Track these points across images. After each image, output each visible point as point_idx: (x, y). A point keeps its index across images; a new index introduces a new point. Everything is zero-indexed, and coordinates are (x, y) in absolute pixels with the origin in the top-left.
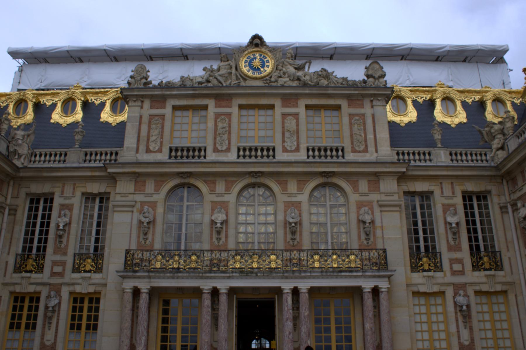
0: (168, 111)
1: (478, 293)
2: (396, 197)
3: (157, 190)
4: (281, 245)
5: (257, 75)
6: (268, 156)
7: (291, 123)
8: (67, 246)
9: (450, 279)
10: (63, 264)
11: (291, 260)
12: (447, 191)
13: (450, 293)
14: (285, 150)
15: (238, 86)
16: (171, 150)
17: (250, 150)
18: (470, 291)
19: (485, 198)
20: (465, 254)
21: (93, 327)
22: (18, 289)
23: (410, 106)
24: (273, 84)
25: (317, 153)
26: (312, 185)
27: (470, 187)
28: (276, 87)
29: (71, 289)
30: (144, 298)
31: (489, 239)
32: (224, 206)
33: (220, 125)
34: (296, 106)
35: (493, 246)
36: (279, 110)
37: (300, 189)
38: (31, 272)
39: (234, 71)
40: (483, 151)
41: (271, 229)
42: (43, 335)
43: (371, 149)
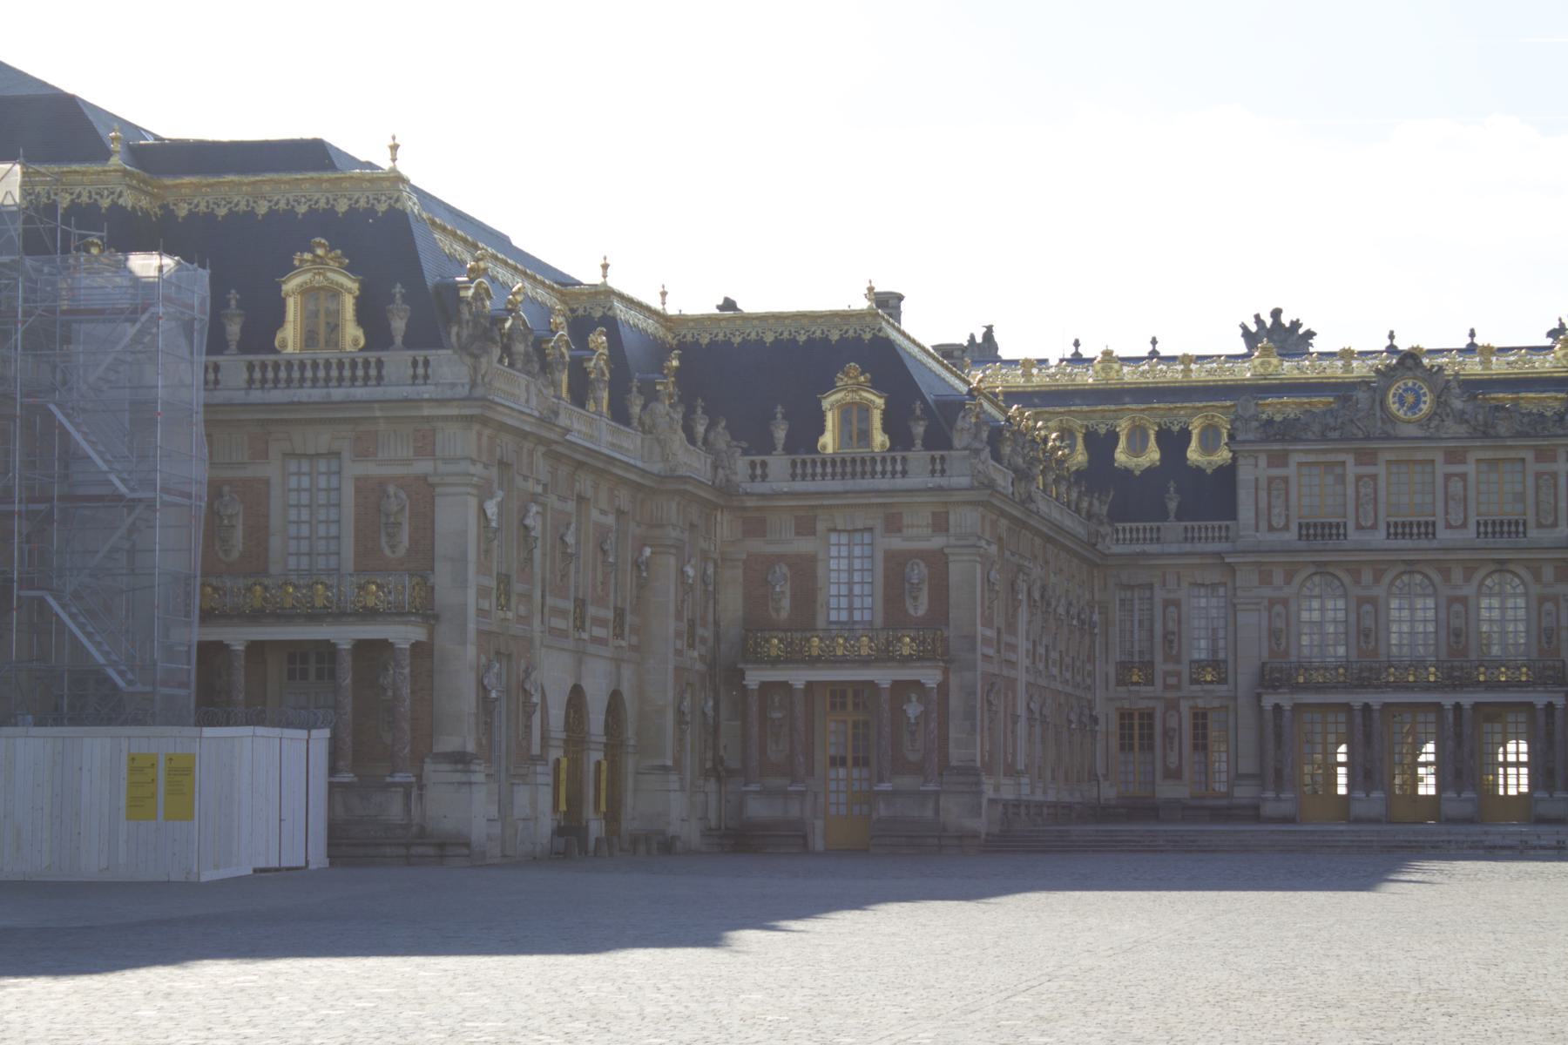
5: (1410, 416)
6: (1427, 534)
7: (1456, 487)
11: (1452, 668)
14: (1449, 526)
15: (1388, 437)
17: (1404, 525)
22: (1127, 706)
25: (1490, 529)
29: (1191, 703)
32: (1373, 601)
33: (1363, 491)
34: (1463, 462)
36: (1441, 469)
37: (1467, 579)
38: (1137, 684)
39: (1378, 408)
42: (1165, 757)
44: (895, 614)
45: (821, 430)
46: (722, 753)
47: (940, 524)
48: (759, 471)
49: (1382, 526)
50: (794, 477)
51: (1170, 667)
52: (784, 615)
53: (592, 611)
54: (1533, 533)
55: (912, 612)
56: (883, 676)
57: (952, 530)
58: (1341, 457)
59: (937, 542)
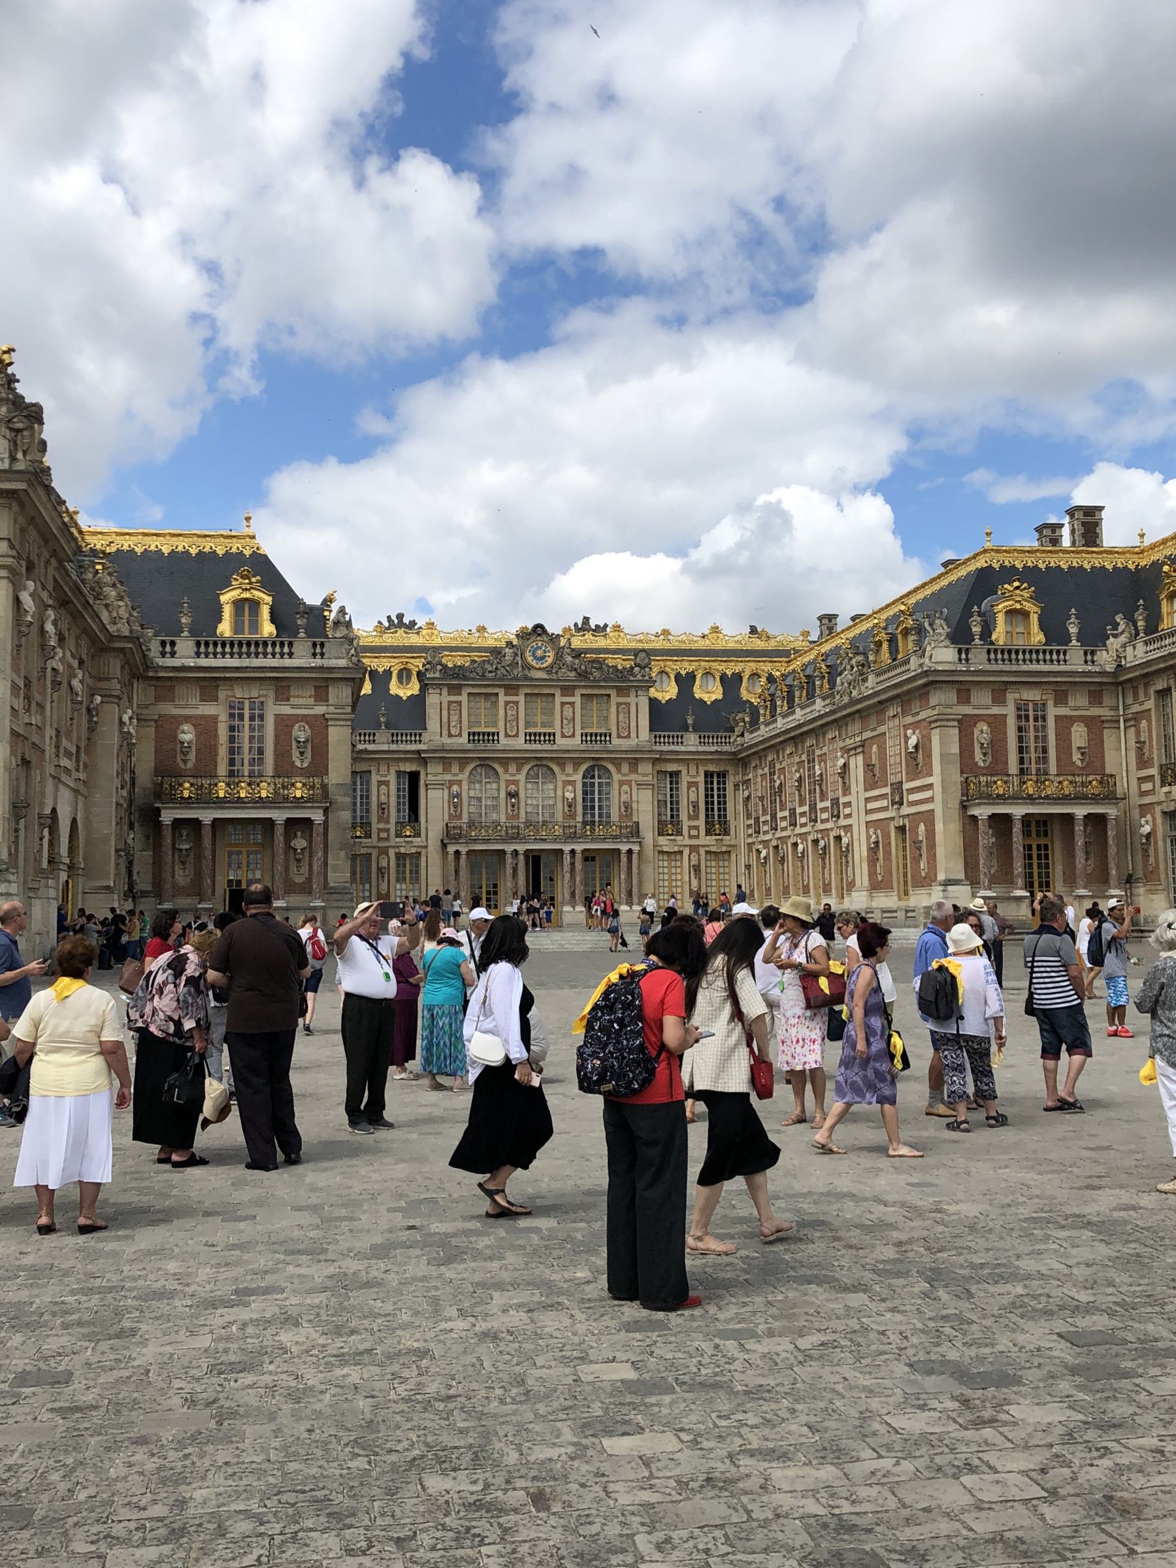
0: (464, 698)
1: (707, 852)
2: (650, 777)
3: (461, 770)
4: (559, 817)
7: (568, 711)
8: (389, 815)
9: (687, 841)
10: (388, 830)
12: (693, 771)
13: (686, 852)
14: (563, 736)
16: (469, 734)
17: (535, 735)
18: (702, 851)
19: (724, 776)
20: (701, 822)
21: (415, 878)
23: (673, 683)
24: (555, 677)
26: (584, 767)
27: (712, 768)
28: (558, 680)
30: (463, 858)
31: (723, 809)
32: (516, 783)
33: (509, 712)
35: (725, 816)
36: (559, 699)
37: (575, 770)
39: (518, 658)
40: (728, 734)
41: (551, 802)
43: (633, 735)
44: (284, 769)
45: (220, 621)
46: (135, 877)
47: (321, 695)
48: (168, 649)
49: (522, 735)
50: (198, 654)
51: (382, 826)
52: (190, 765)
53: (65, 743)
54: (615, 741)
55: (298, 764)
56: (279, 816)
57: (330, 702)
58: (496, 690)
59: (320, 710)
